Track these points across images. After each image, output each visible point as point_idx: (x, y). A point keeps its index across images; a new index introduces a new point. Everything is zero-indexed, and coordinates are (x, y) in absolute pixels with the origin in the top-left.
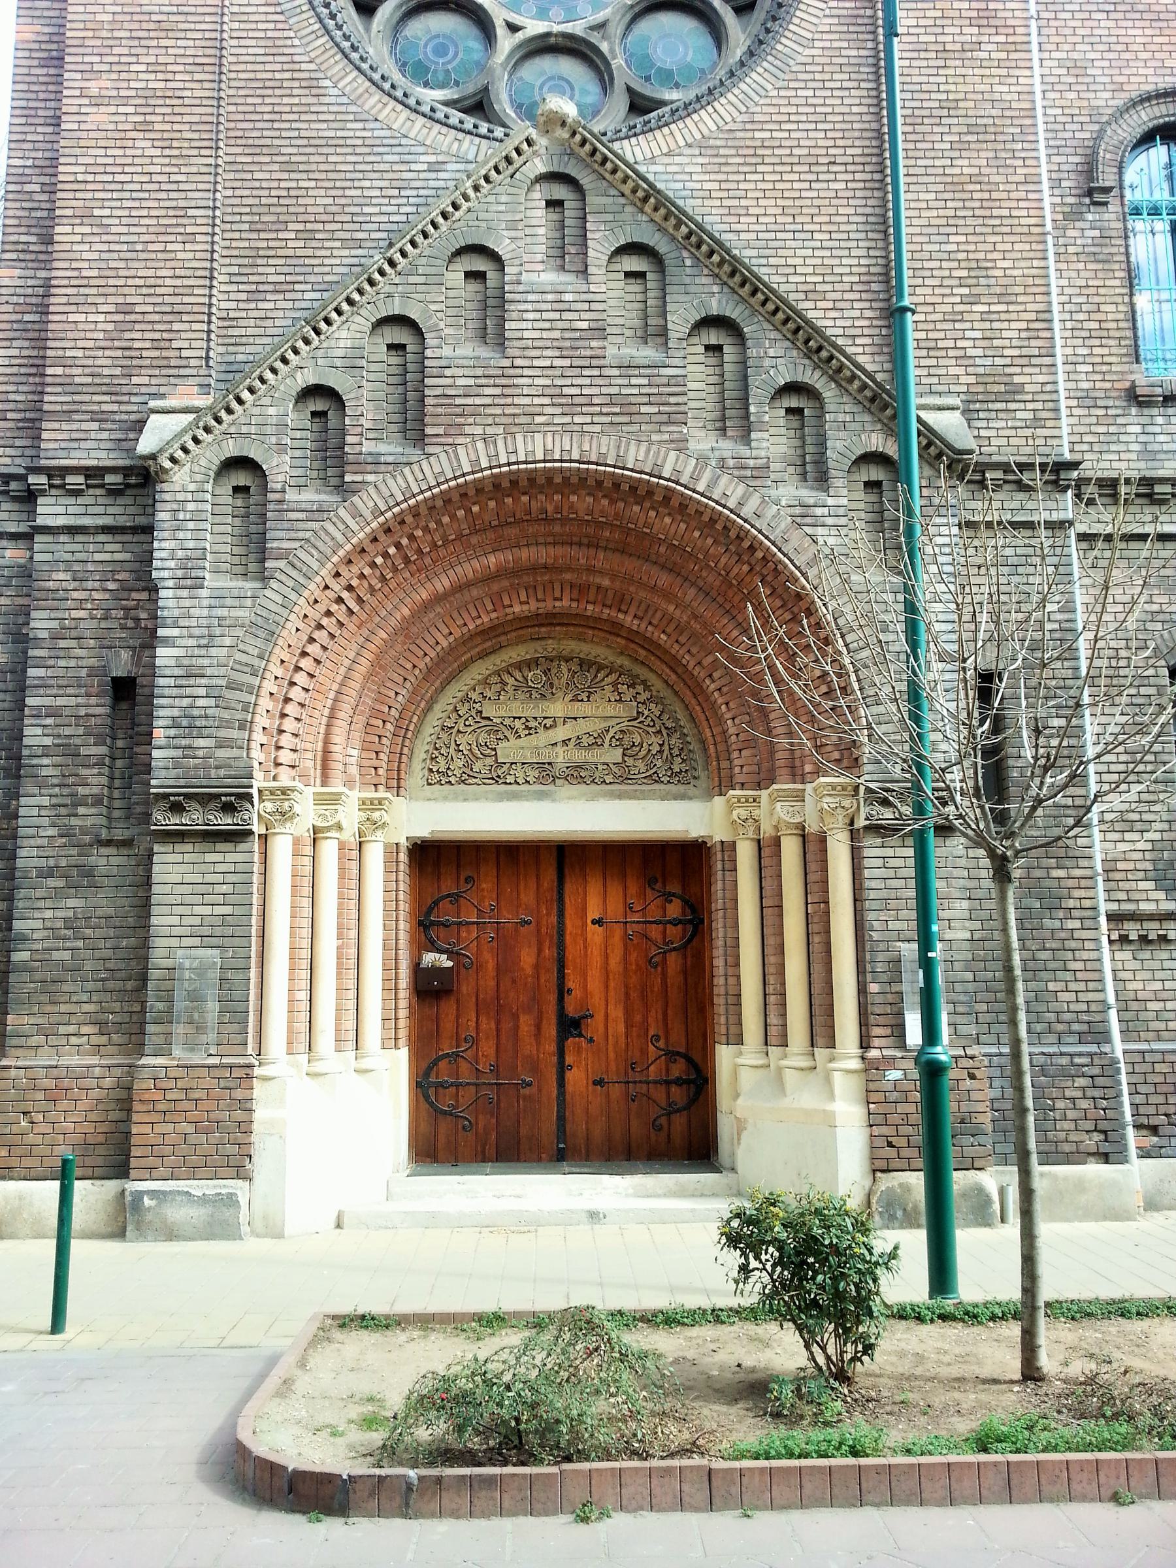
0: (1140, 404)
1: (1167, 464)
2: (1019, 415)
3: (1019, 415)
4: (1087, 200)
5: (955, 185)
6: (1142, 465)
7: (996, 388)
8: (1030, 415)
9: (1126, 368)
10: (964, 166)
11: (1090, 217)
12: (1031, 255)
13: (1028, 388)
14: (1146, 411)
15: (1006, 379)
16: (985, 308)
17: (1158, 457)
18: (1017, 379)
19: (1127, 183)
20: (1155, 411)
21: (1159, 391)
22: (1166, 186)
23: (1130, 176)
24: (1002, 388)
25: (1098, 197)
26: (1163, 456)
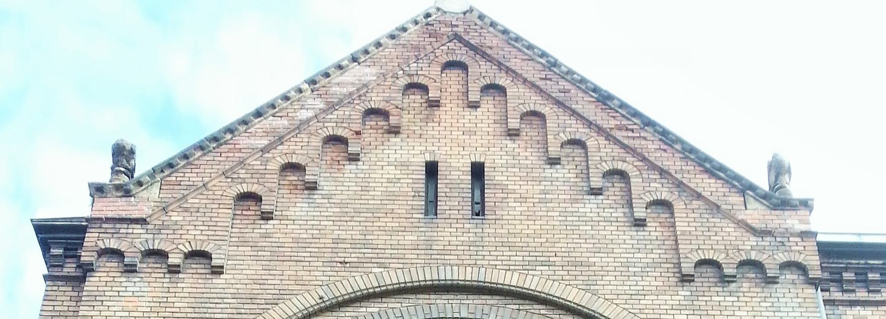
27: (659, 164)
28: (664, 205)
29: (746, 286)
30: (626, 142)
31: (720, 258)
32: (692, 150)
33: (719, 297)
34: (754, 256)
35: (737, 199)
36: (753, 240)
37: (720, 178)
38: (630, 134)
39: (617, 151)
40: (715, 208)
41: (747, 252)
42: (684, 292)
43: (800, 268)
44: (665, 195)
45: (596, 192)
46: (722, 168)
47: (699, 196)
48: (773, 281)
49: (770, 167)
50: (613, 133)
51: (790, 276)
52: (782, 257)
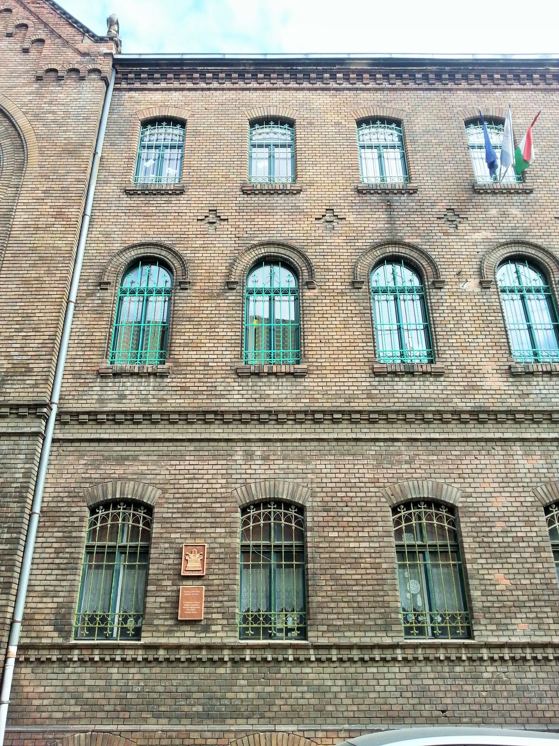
0: (102, 377)
1: (109, 405)
2: (28, 382)
3: (28, 382)
4: (99, 288)
5: (26, 282)
6: (98, 405)
7: (20, 370)
8: (33, 382)
9: (100, 360)
10: (33, 274)
11: (98, 295)
12: (53, 311)
13: (35, 370)
14: (104, 380)
15: (26, 366)
16: (25, 334)
17: (106, 401)
18: (31, 366)
19: (498, 280)
20: (109, 380)
21: (110, 371)
22: (517, 281)
23: (499, 276)
24: (23, 370)
25: (103, 286)
26: (108, 401)
27: (45, 20)
28: (42, 41)
29: (70, 83)
30: (33, 9)
31: (58, 68)
32: (65, 13)
33: (53, 88)
34: (76, 66)
35: (79, 38)
36: (79, 58)
37: (75, 27)
38: (38, 5)
39: (27, 14)
40: (66, 43)
41: (74, 64)
42: (36, 86)
43: (98, 71)
44: (43, 37)
45: (9, 35)
46: (76, 22)
47: (60, 37)
48: (82, 79)
49: (108, 21)
50: (28, 6)
51: (93, 76)
52: (91, 67)
